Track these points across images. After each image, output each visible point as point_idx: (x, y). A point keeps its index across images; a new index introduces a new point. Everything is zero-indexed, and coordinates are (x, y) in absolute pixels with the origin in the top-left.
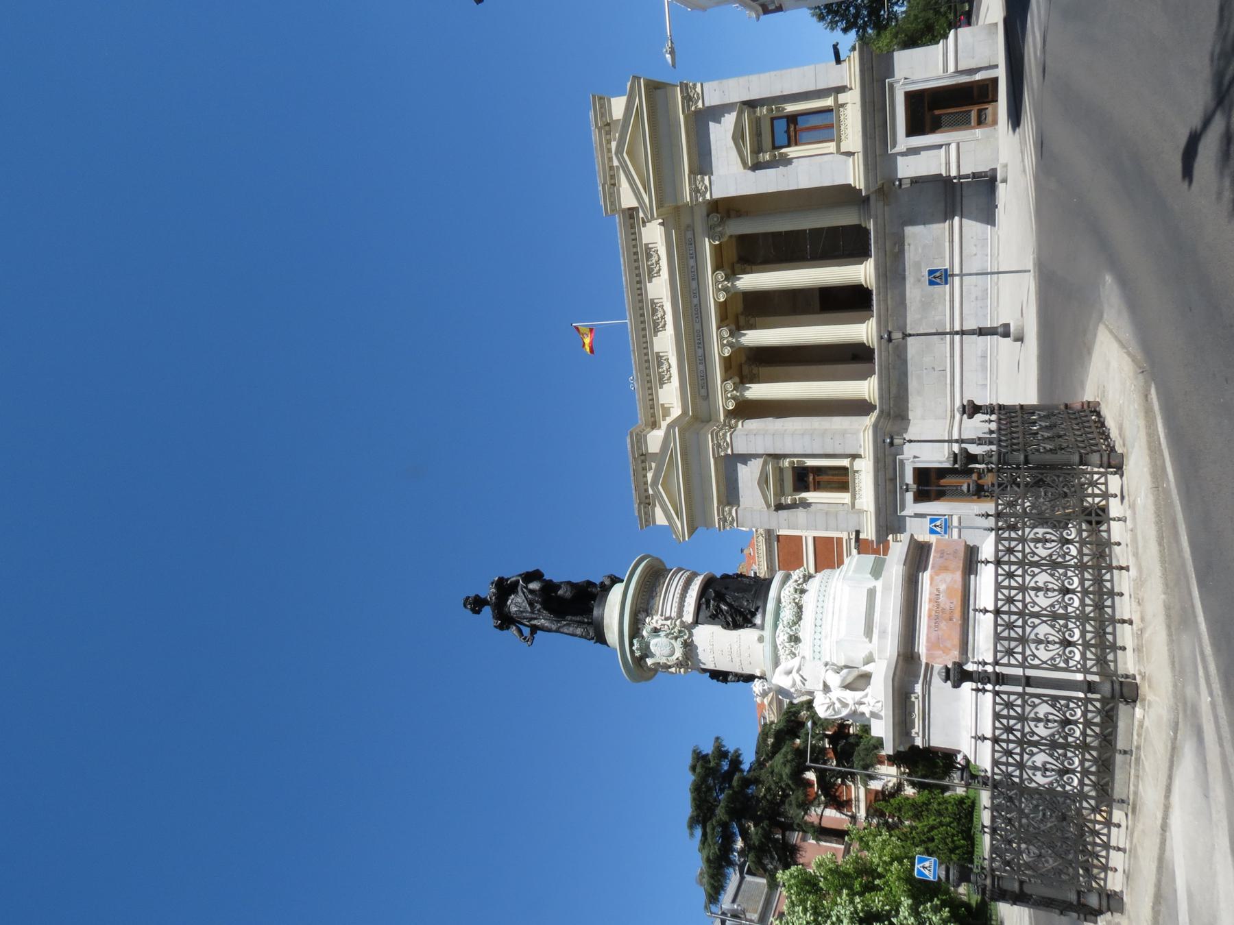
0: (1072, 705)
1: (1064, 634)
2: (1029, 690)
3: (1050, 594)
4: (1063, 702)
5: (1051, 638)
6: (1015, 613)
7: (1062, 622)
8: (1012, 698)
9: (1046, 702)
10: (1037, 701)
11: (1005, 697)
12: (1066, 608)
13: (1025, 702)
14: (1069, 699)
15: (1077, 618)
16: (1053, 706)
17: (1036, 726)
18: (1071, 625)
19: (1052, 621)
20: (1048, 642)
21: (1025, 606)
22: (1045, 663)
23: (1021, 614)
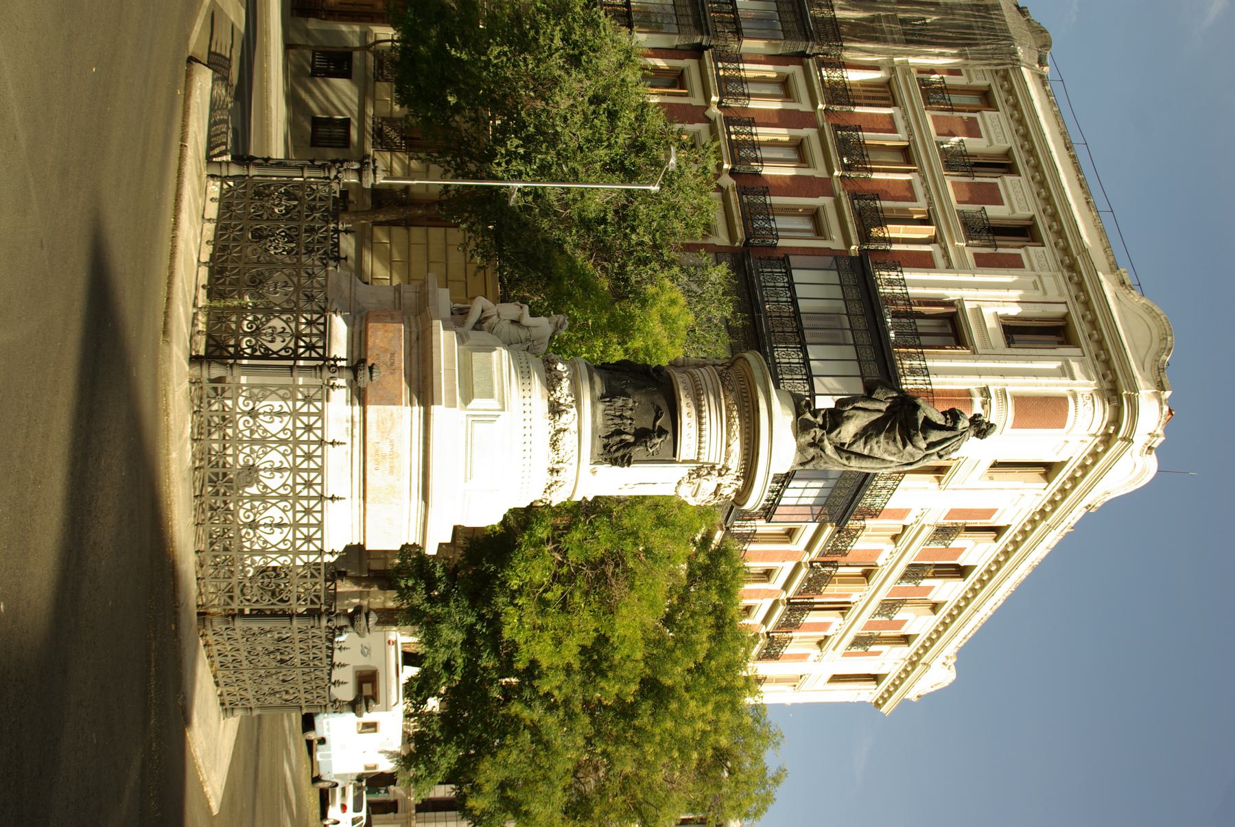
0: (248, 351)
1: (255, 424)
2: (291, 363)
3: (268, 465)
4: (258, 353)
5: (267, 418)
6: (304, 442)
7: (256, 436)
8: (307, 354)
9: (274, 353)
10: (283, 353)
11: (314, 355)
12: (252, 451)
13: (295, 351)
14: (252, 357)
15: (241, 441)
16: (267, 349)
17: (284, 328)
18: (247, 433)
19: (265, 437)
20: (270, 413)
21: (293, 451)
22: (273, 392)
23: (297, 442)
